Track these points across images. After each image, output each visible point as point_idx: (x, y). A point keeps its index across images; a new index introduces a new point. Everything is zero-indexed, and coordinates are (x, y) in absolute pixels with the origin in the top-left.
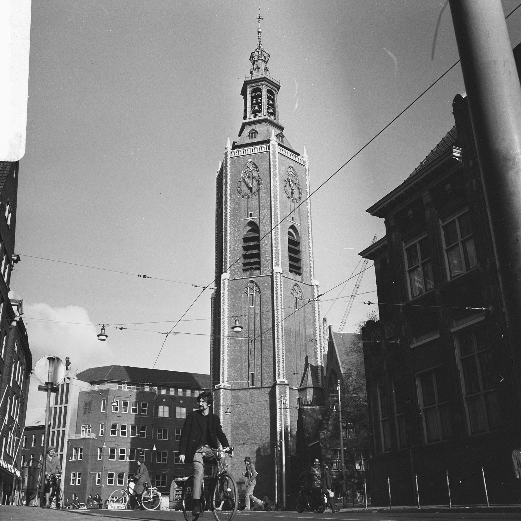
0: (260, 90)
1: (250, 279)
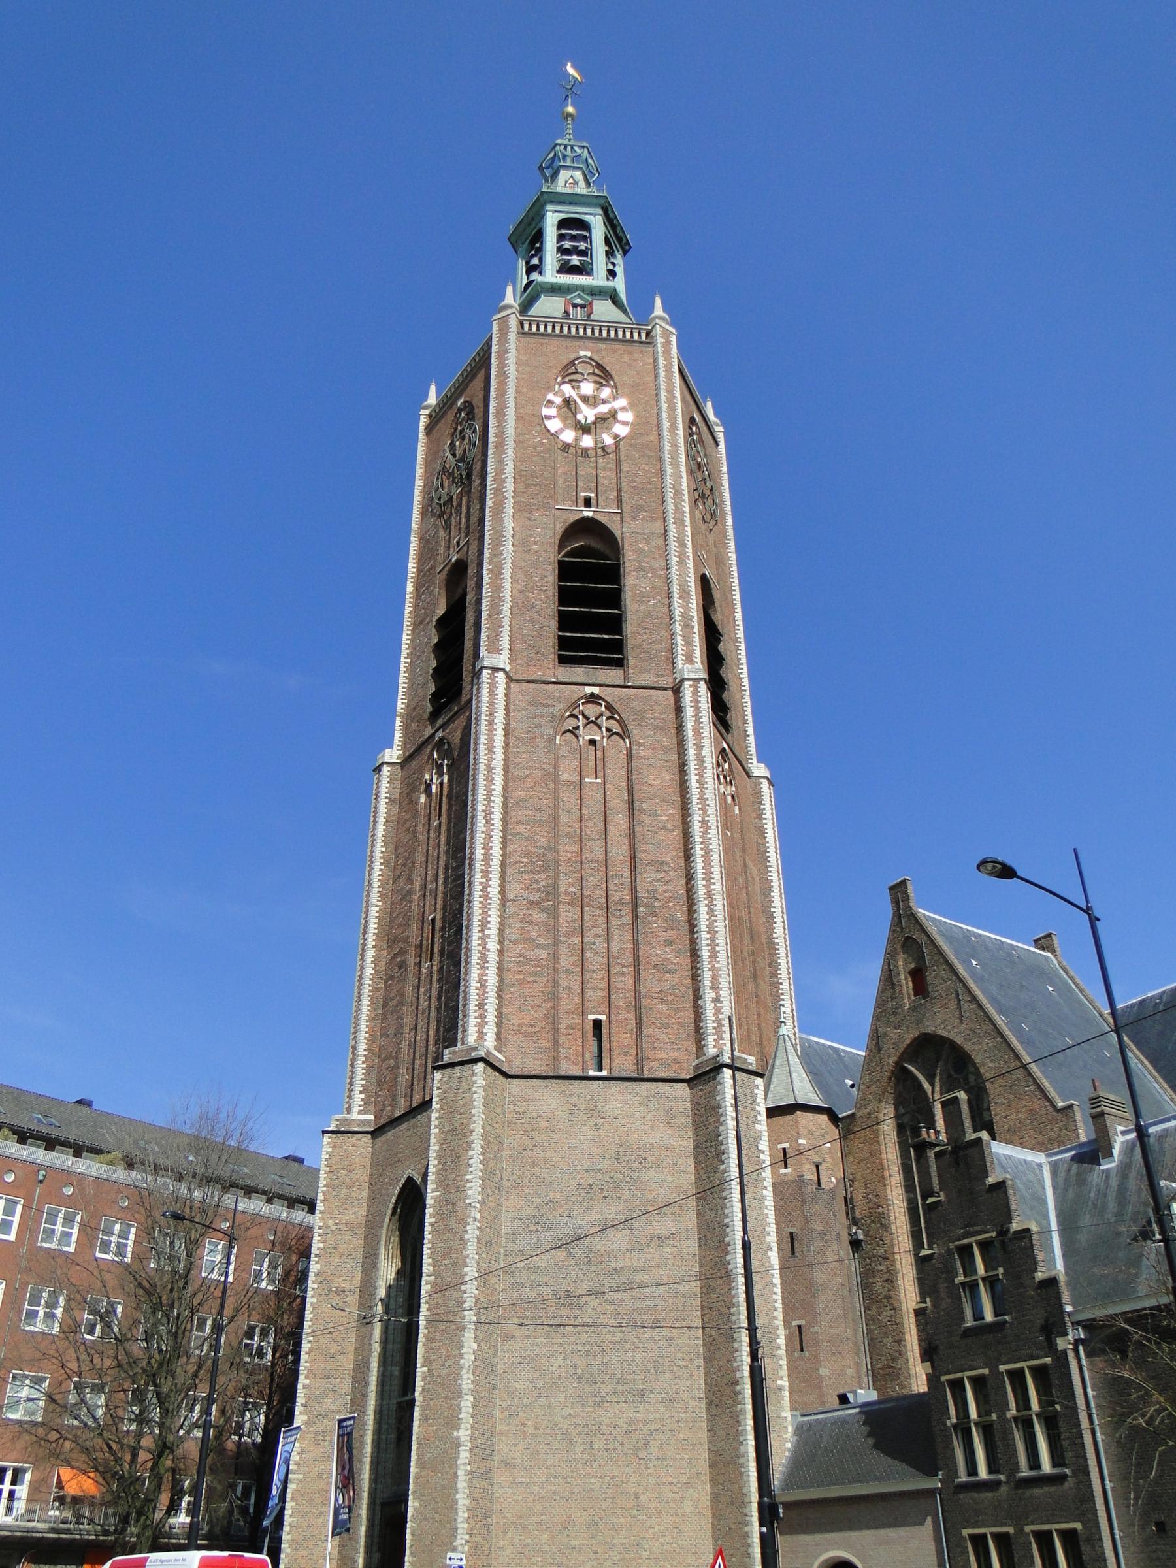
0: (584, 225)
1: (589, 690)
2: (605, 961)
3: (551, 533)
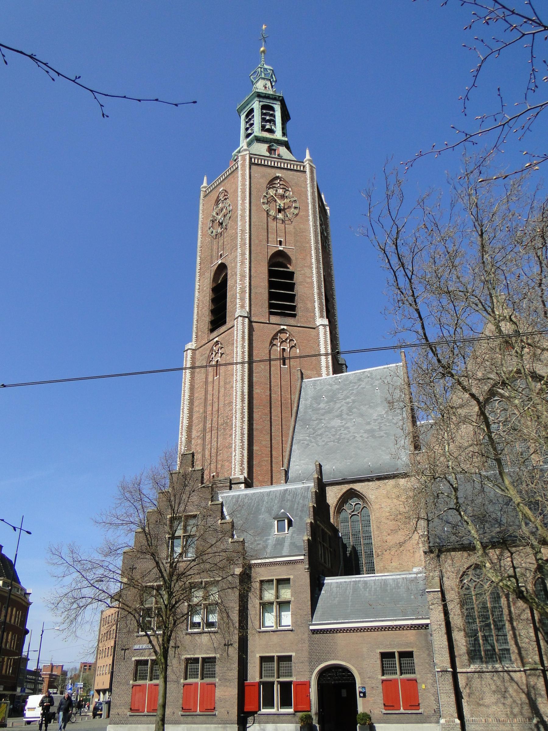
1: (215, 340)
3: (209, 279)
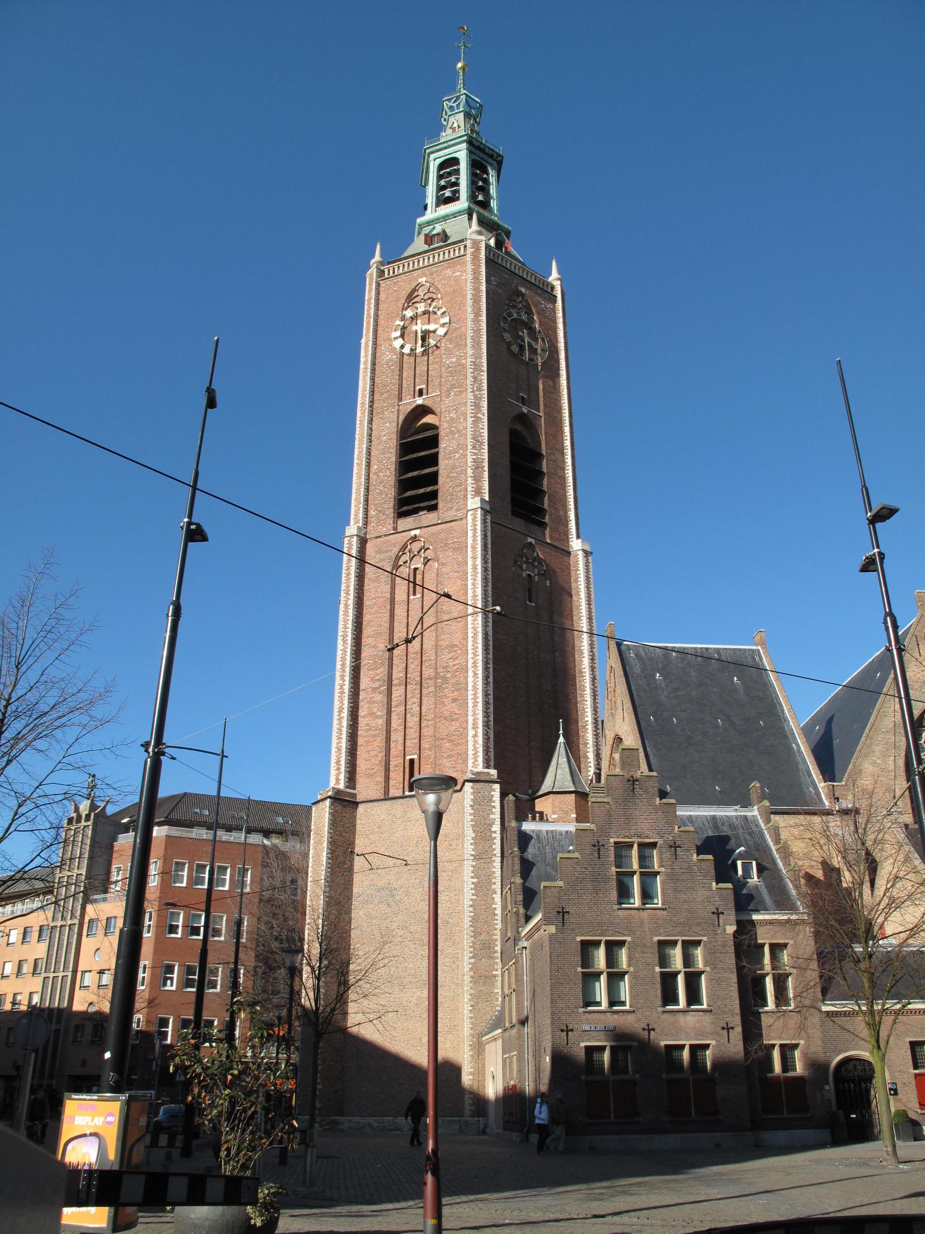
0: (454, 161)
1: (413, 533)
2: (418, 719)
3: (395, 425)
